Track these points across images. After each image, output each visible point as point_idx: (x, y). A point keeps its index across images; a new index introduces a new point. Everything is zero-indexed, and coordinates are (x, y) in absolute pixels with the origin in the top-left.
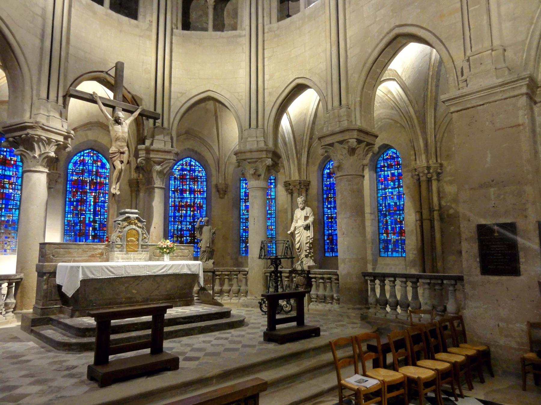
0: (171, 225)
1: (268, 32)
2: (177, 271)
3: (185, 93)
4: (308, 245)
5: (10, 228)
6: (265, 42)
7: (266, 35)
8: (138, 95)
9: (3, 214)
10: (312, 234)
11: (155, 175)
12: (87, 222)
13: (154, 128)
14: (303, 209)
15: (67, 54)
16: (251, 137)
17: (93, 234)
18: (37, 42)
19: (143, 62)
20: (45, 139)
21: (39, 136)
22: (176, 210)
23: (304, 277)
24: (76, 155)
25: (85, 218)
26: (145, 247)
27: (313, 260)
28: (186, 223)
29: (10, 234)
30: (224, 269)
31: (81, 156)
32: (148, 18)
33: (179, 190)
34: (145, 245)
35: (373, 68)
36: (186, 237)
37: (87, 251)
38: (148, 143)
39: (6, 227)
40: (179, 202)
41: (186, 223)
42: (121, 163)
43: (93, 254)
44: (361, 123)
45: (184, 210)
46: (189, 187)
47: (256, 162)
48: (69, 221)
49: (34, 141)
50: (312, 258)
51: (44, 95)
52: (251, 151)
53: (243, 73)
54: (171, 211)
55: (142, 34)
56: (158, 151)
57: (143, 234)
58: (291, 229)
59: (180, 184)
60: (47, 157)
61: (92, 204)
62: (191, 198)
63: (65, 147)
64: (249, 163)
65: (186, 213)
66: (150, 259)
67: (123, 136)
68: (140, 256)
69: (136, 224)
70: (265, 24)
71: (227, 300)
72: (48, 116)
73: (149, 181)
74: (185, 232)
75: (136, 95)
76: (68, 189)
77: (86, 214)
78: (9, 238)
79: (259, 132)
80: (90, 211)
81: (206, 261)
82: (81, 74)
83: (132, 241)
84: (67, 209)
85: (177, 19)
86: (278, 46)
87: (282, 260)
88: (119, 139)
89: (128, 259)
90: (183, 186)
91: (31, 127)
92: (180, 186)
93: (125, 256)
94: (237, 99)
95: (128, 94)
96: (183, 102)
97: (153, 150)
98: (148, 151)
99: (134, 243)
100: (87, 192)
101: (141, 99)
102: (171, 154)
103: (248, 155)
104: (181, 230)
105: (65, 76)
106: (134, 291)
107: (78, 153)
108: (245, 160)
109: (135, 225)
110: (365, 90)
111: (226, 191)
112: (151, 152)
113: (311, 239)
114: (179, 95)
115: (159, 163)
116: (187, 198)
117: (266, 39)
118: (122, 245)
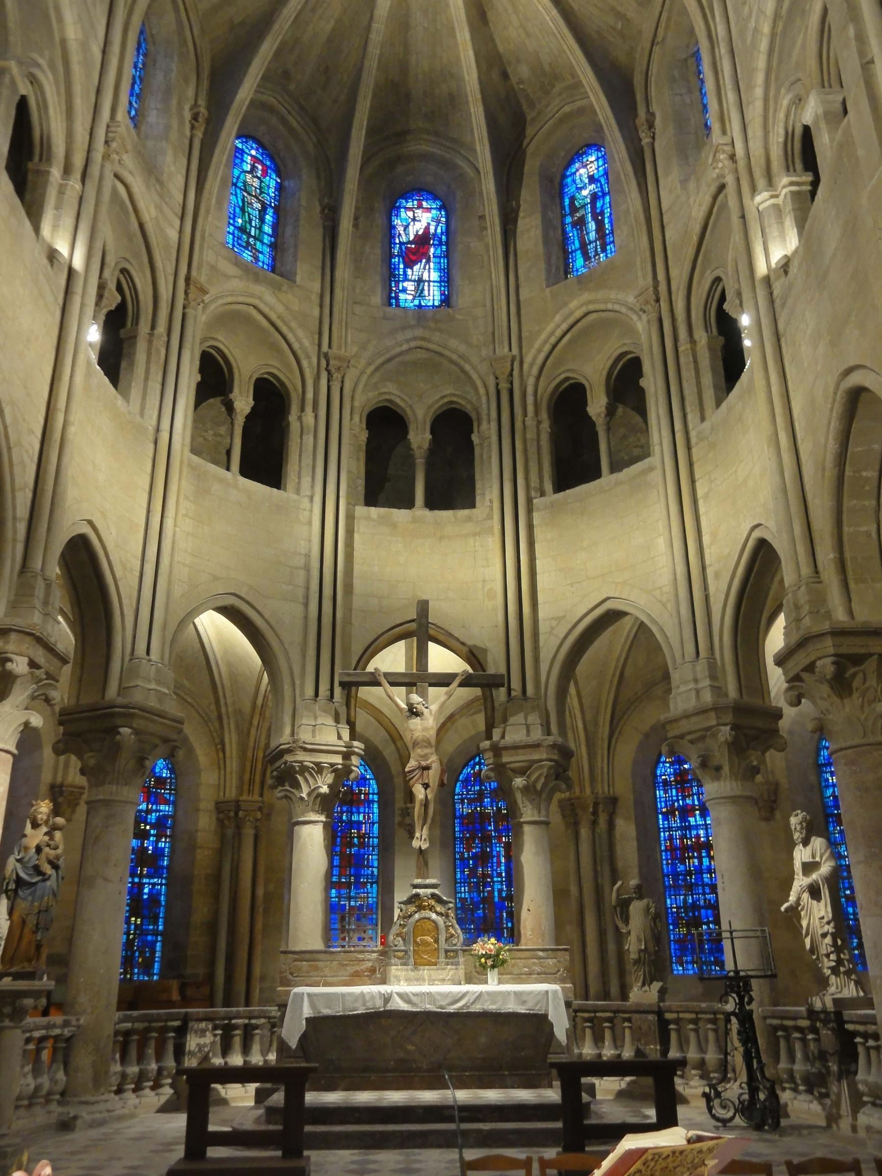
0: (670, 896)
1: (697, 444)
2: (492, 1007)
3: (564, 617)
4: (828, 940)
5: (364, 921)
6: (696, 467)
7: (694, 451)
8: (480, 644)
9: (352, 894)
10: (829, 909)
11: (519, 796)
12: (496, 899)
13: (508, 702)
14: (806, 842)
15: (349, 609)
16: (686, 683)
17: (510, 925)
18: (300, 609)
19: (484, 581)
20: (312, 765)
21: (301, 762)
22: (677, 859)
23: (832, 1030)
24: (466, 765)
25: (491, 893)
26: (451, 955)
27: (857, 983)
28: (704, 890)
29: (365, 932)
30: (681, 1006)
31: (475, 764)
32: (487, 498)
33: (677, 809)
34: (453, 951)
35: (848, 472)
36: (707, 924)
37: (347, 965)
38: (496, 734)
39: (358, 919)
40: (681, 839)
41: (704, 890)
42: (426, 789)
43: (357, 971)
44: (851, 613)
45: (693, 857)
46: (699, 799)
47: (703, 738)
49: (296, 772)
50: (853, 977)
51: (310, 692)
52: (687, 716)
53: (661, 543)
54: (665, 862)
55: (478, 530)
56: (516, 747)
57: (447, 927)
58: (791, 898)
59: (677, 796)
60: (319, 795)
61: (503, 860)
62: (706, 825)
63: (347, 770)
64: (692, 742)
65: (701, 863)
66: (469, 980)
67: (424, 736)
68: (442, 974)
69: (432, 908)
70: (691, 427)
71: (695, 1087)
72: (315, 726)
73: (513, 811)
74: (703, 911)
75: (475, 646)
76: (457, 835)
77: (494, 882)
78: (364, 939)
79: (702, 667)
80: (500, 875)
81: (643, 985)
82: (375, 636)
83: (427, 944)
84: (458, 876)
86: (717, 466)
87: (754, 982)
88: (418, 744)
89: (417, 980)
90: (684, 799)
91: (289, 751)
92: (678, 801)
93: (412, 974)
94: (660, 602)
95: (461, 646)
96: (562, 635)
97: (506, 748)
98: (497, 750)
99: (429, 948)
100: (491, 837)
101: (485, 651)
102: (541, 749)
103: (685, 726)
104: (695, 906)
106: (410, 1047)
107: (470, 761)
108: (682, 737)
109: (431, 910)
110: (846, 529)
111: (774, 802)
112: (504, 752)
113: (828, 923)
114: (554, 623)
115: (522, 772)
116: (697, 827)
117: (695, 458)
118: (406, 952)
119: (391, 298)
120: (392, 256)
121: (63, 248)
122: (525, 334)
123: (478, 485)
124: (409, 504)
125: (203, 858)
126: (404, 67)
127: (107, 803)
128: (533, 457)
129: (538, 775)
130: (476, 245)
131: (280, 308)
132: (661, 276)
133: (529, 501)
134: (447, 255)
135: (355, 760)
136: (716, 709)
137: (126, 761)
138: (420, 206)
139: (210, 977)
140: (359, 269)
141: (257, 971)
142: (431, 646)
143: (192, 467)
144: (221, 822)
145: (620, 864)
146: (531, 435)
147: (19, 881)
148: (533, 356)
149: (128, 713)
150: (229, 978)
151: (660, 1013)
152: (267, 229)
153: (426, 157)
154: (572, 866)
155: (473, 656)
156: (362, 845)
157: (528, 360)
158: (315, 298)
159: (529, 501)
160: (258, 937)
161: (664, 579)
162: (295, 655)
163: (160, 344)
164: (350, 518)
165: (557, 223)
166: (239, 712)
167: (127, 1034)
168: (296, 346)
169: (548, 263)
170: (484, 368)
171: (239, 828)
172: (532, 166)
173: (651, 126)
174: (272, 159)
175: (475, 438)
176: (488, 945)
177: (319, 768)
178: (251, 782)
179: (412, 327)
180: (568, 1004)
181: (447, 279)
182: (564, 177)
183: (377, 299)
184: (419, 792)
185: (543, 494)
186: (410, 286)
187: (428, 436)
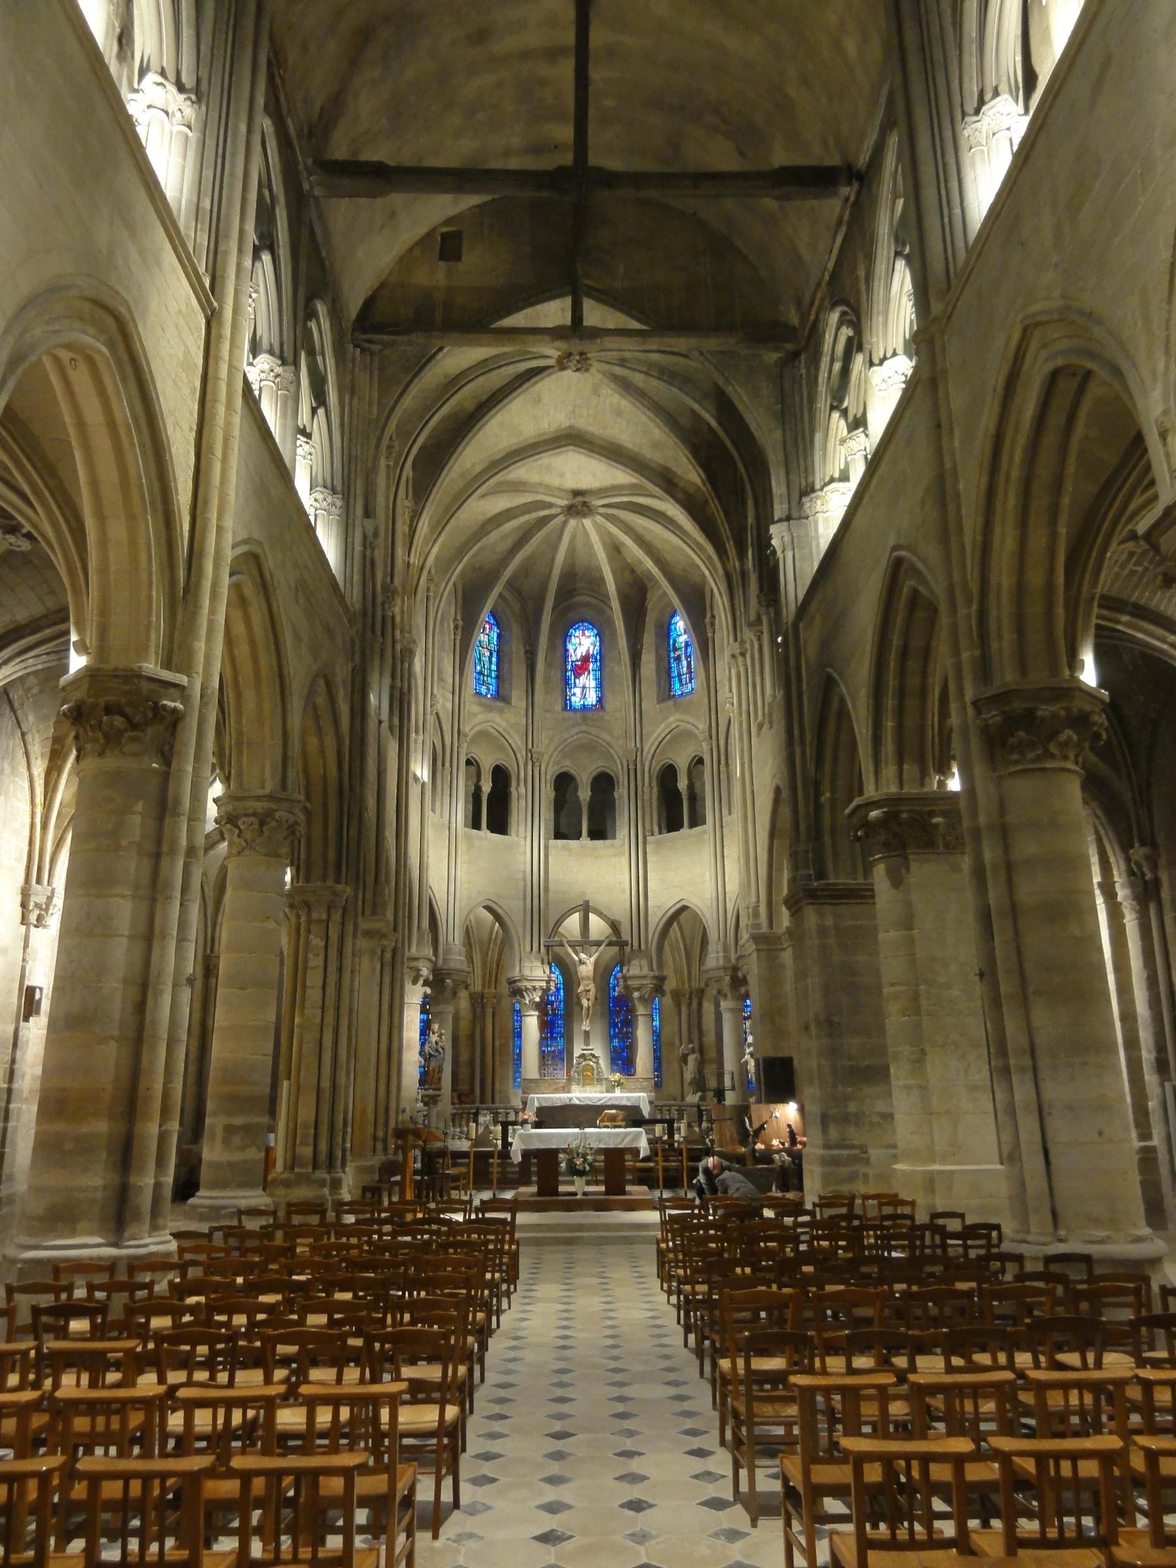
11: (636, 1002)
18: (521, 902)
26: (600, 1080)
38: (625, 969)
48: (615, 1047)
51: (528, 948)
52: (712, 969)
56: (634, 977)
63: (548, 989)
66: (608, 1091)
73: (631, 1010)
79: (720, 947)
85: (652, 824)
98: (625, 978)
103: (712, 974)
108: (710, 979)
115: (638, 989)
119: (566, 705)
120: (566, 670)
121: (419, 774)
122: (644, 732)
123: (618, 824)
124: (578, 836)
125: (465, 1025)
126: (573, 565)
127: (441, 1013)
128: (647, 810)
129: (647, 991)
131: (504, 724)
132: (713, 724)
134: (601, 669)
135: (552, 984)
136: (724, 968)
137: (448, 994)
138: (584, 634)
139: (472, 1090)
140: (548, 690)
142: (591, 915)
143: (465, 835)
144: (473, 1005)
145: (705, 1028)
146: (646, 797)
147: (430, 1055)
148: (649, 746)
149: (449, 974)
150: (483, 1091)
151: (698, 1107)
152: (494, 667)
154: (677, 1029)
155: (614, 926)
156: (554, 1014)
157: (646, 749)
158: (523, 712)
161: (708, 895)
162: (520, 930)
163: (447, 772)
164: (547, 847)
165: (665, 655)
167: (454, 1115)
168: (513, 745)
169: (659, 686)
170: (621, 753)
171: (483, 1008)
172: (651, 619)
173: (713, 625)
174: (495, 619)
175: (616, 794)
176: (617, 1076)
177: (535, 989)
178: (490, 981)
179: (579, 725)
180: (651, 1103)
181: (600, 686)
182: (670, 624)
183: (559, 707)
184: (585, 1003)
185: (652, 834)
186: (578, 691)
187: (590, 793)
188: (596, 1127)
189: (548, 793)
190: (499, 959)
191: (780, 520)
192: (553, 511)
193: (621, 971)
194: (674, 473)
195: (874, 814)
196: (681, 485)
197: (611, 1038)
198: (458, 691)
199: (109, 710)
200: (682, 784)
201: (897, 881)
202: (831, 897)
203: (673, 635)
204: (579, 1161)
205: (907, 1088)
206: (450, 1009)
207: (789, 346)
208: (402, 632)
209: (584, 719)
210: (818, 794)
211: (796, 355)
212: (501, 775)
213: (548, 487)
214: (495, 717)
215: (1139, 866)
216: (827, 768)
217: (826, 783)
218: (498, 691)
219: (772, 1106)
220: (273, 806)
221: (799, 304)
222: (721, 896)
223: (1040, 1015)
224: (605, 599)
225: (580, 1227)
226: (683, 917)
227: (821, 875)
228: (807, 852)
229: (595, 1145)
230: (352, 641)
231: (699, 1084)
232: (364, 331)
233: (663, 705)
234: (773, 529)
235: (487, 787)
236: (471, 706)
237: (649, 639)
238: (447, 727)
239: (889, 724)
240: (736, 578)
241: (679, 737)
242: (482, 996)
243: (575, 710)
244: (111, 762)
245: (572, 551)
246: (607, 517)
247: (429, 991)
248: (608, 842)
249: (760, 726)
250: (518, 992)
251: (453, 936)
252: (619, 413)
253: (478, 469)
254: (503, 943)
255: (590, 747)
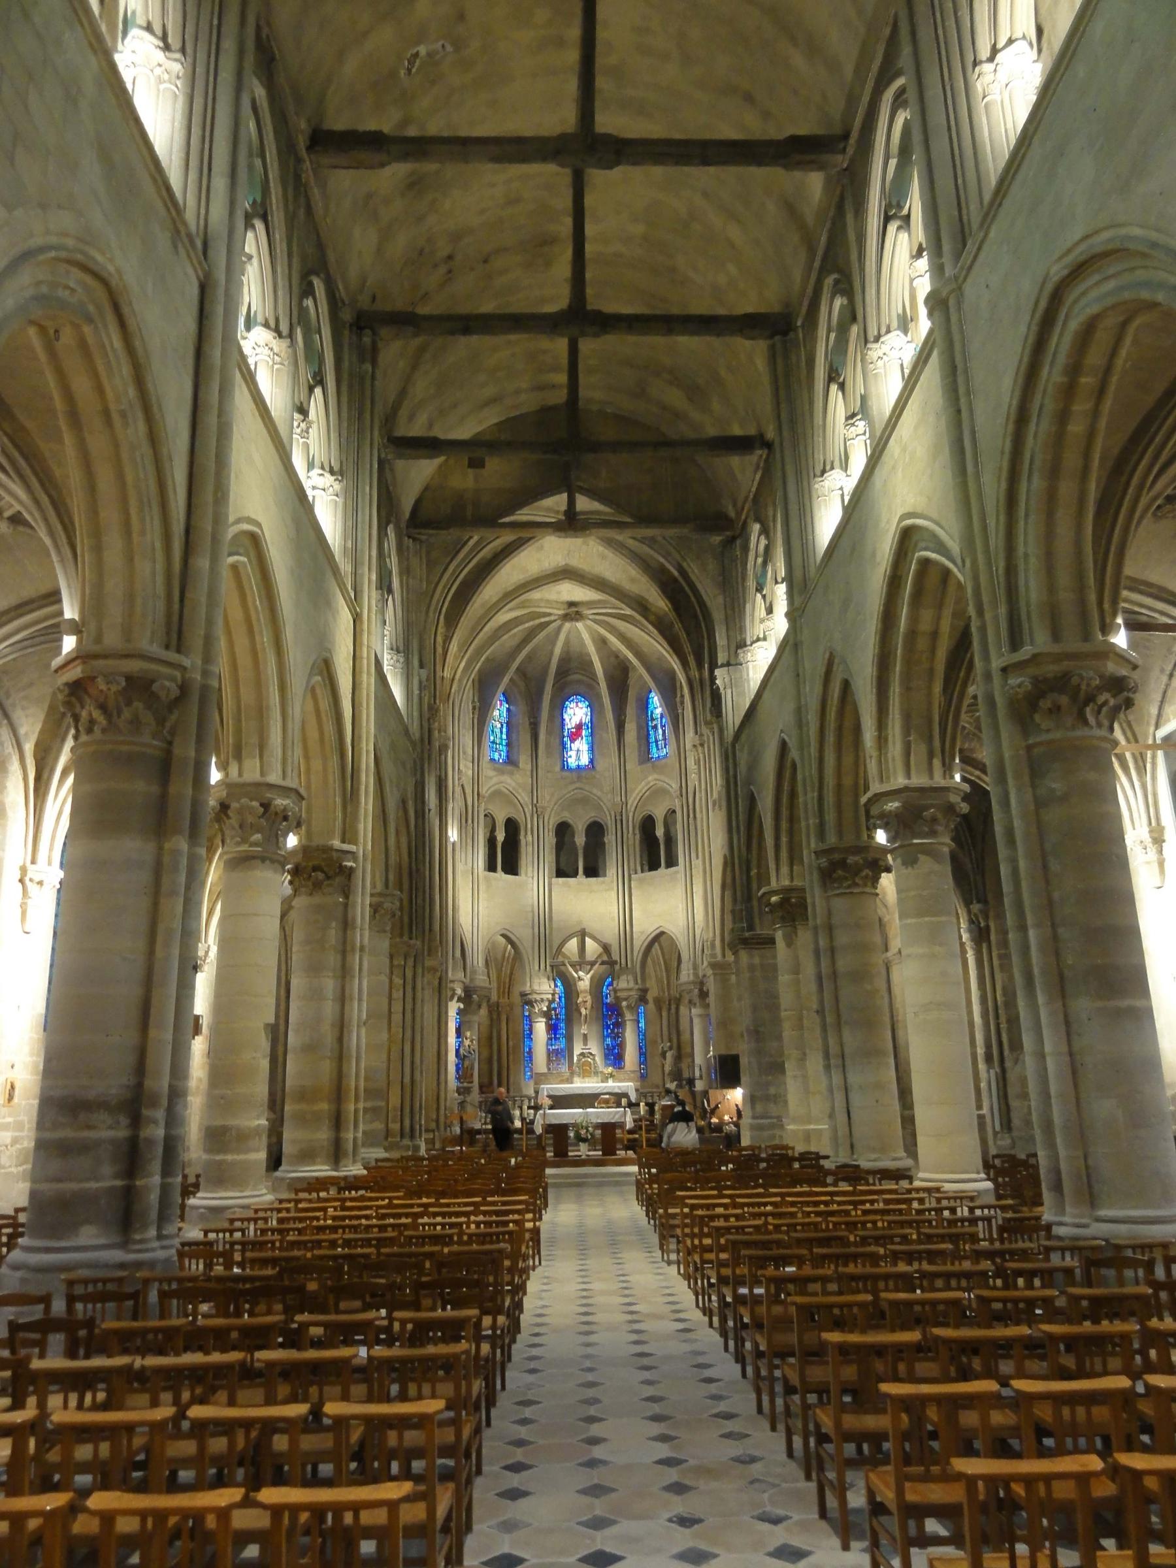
15: (551, 928)
26: (596, 1073)
38: (615, 983)
51: (537, 968)
53: (681, 907)
63: (553, 1001)
73: (620, 1014)
79: (691, 966)
98: (615, 991)
103: (684, 988)
105: (551, 947)
115: (626, 999)
119: (564, 766)
128: (631, 851)
129: (633, 1002)
130: (605, 735)
131: (514, 784)
133: (630, 876)
134: (592, 735)
136: (693, 983)
137: (474, 1006)
140: (549, 754)
141: (511, 1080)
142: (587, 939)
146: (631, 842)
148: (632, 801)
152: (504, 737)
153: (579, 682)
154: (658, 1028)
155: (606, 948)
156: (557, 1019)
158: (529, 773)
159: (630, 876)
160: (511, 1066)
162: (530, 951)
166: (496, 959)
169: (640, 751)
171: (499, 1015)
172: (632, 695)
176: (610, 1069)
177: (542, 1000)
180: (637, 1090)
181: (592, 749)
182: (648, 698)
183: (558, 768)
184: (583, 1011)
188: (594, 1107)
189: (550, 840)
190: (511, 974)
191: (722, 666)
192: (552, 618)
193: (611, 984)
194: (647, 600)
195: (774, 899)
196: (653, 609)
197: (604, 1038)
198: (477, 761)
199: (315, 869)
200: (660, 832)
201: (790, 943)
202: (758, 943)
203: (651, 707)
204: (583, 1132)
205: (795, 1077)
206: (476, 1018)
207: (728, 533)
208: (439, 731)
209: (579, 778)
210: (748, 870)
211: (733, 539)
212: (512, 827)
213: (548, 601)
214: (506, 778)
215: (975, 915)
216: (754, 852)
217: (754, 863)
218: (508, 756)
219: (725, 1091)
220: (382, 899)
221: (735, 505)
222: (691, 925)
223: (847, 1034)
224: (593, 676)
225: (585, 1176)
226: (662, 939)
227: (751, 927)
228: (741, 910)
229: (594, 1121)
230: (415, 762)
231: (677, 1075)
232: (416, 527)
233: (644, 766)
234: (717, 672)
235: (501, 836)
236: (487, 771)
237: (631, 711)
238: (468, 791)
239: (784, 839)
240: (696, 685)
241: (657, 793)
242: (498, 1004)
243: (570, 770)
244: (317, 899)
245: (567, 642)
246: (595, 621)
247: (462, 1006)
248: (600, 879)
249: (714, 805)
250: (530, 1003)
251: (478, 959)
252: (604, 557)
253: (495, 599)
254: (514, 959)
255: (584, 801)
